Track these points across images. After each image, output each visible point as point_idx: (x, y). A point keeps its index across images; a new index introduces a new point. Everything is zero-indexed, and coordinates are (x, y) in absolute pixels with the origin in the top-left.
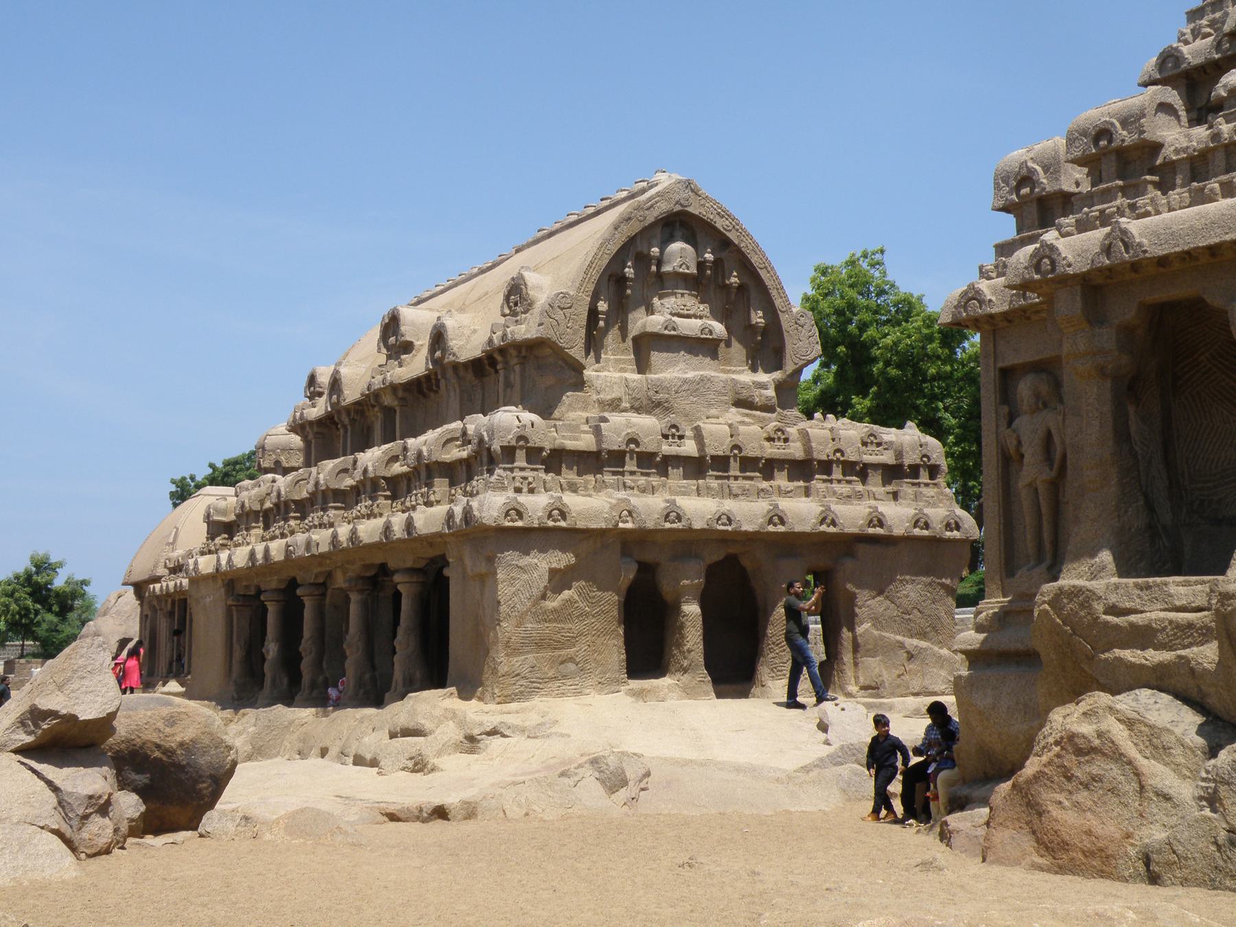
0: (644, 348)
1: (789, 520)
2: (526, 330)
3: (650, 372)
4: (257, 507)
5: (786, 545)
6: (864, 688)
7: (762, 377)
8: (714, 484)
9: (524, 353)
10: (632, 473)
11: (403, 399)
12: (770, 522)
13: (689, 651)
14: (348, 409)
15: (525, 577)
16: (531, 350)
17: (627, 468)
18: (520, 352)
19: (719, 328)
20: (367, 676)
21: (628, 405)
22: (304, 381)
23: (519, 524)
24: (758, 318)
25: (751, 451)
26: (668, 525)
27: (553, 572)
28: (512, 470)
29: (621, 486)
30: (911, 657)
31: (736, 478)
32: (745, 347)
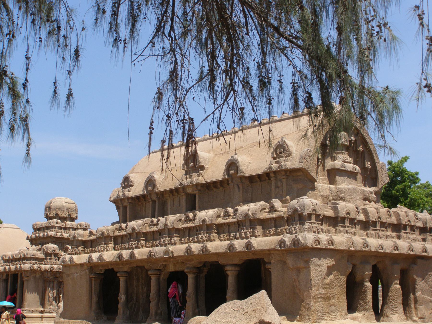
0: (333, 175)
1: (400, 248)
2: (291, 163)
3: (336, 184)
4: (111, 234)
5: (395, 258)
6: (420, 318)
7: (372, 189)
8: (373, 232)
9: (288, 173)
10: (348, 227)
11: (200, 190)
12: (394, 249)
13: (369, 302)
14: (157, 194)
15: (320, 269)
16: (291, 173)
17: (346, 224)
18: (286, 173)
19: (358, 168)
21: (332, 198)
22: (121, 180)
23: (319, 246)
24: (368, 164)
25: (384, 220)
26: (364, 249)
27: (328, 267)
29: (345, 232)
31: (379, 230)
32: (362, 176)
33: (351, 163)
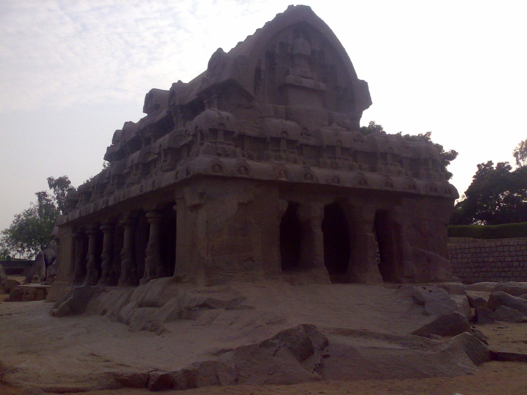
20: (132, 270)
28: (215, 143)
30: (429, 260)
33: (313, 79)
